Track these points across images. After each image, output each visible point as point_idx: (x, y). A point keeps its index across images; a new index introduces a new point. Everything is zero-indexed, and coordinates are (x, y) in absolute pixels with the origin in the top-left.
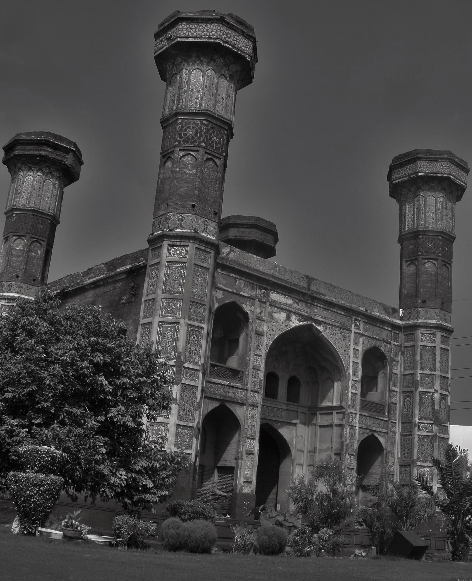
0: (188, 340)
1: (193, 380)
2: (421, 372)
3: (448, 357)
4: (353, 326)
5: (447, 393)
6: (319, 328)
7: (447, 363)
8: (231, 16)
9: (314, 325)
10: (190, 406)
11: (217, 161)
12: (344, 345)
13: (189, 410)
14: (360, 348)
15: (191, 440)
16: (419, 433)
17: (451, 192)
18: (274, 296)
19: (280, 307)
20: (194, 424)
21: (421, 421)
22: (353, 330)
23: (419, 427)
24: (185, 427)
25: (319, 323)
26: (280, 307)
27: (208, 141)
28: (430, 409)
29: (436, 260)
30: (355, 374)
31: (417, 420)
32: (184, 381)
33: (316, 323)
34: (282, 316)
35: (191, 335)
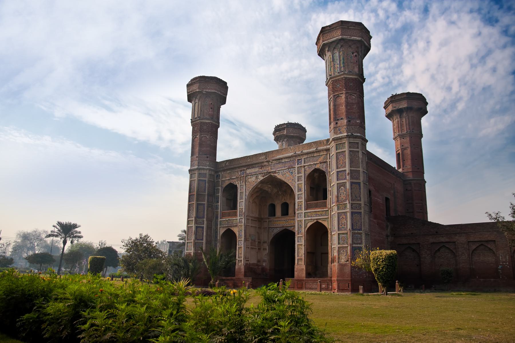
4: (296, 164)
5: (345, 181)
6: (275, 175)
8: (192, 80)
9: (272, 174)
11: (198, 136)
12: (292, 177)
14: (303, 175)
17: (334, 48)
18: (248, 171)
19: (251, 175)
20: (192, 241)
22: (297, 166)
25: (275, 172)
26: (251, 175)
30: (300, 190)
33: (273, 173)
34: (254, 179)
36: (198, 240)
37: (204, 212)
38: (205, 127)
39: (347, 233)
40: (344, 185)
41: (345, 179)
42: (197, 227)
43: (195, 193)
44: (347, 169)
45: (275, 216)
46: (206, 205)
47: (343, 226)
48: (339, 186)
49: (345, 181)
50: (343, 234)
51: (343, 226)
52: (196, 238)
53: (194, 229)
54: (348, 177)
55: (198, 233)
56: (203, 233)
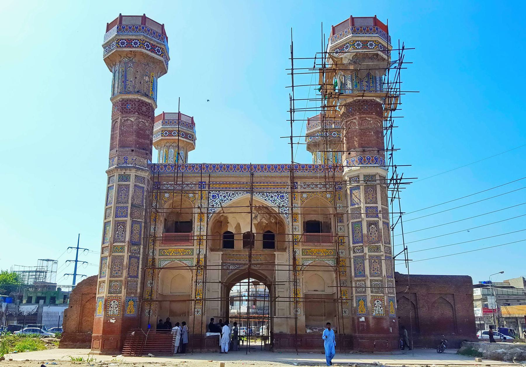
0: (116, 230)
1: (121, 252)
2: (352, 207)
3: (376, 191)
7: (375, 195)
10: (119, 268)
13: (119, 270)
15: (121, 288)
16: (354, 255)
20: (123, 279)
21: (355, 245)
23: (354, 249)
24: (116, 281)
27: (123, 110)
28: (360, 234)
29: (355, 119)
31: (351, 245)
32: (114, 254)
35: (118, 226)
36: (130, 277)
37: (140, 235)
38: (144, 109)
39: (381, 281)
40: (376, 224)
41: (377, 216)
42: (130, 257)
43: (129, 205)
44: (362, 205)
45: (233, 247)
46: (143, 224)
47: (376, 271)
48: (369, 224)
49: (376, 219)
50: (377, 281)
51: (376, 271)
52: (129, 274)
53: (126, 261)
54: (380, 215)
55: (131, 267)
56: (138, 267)
